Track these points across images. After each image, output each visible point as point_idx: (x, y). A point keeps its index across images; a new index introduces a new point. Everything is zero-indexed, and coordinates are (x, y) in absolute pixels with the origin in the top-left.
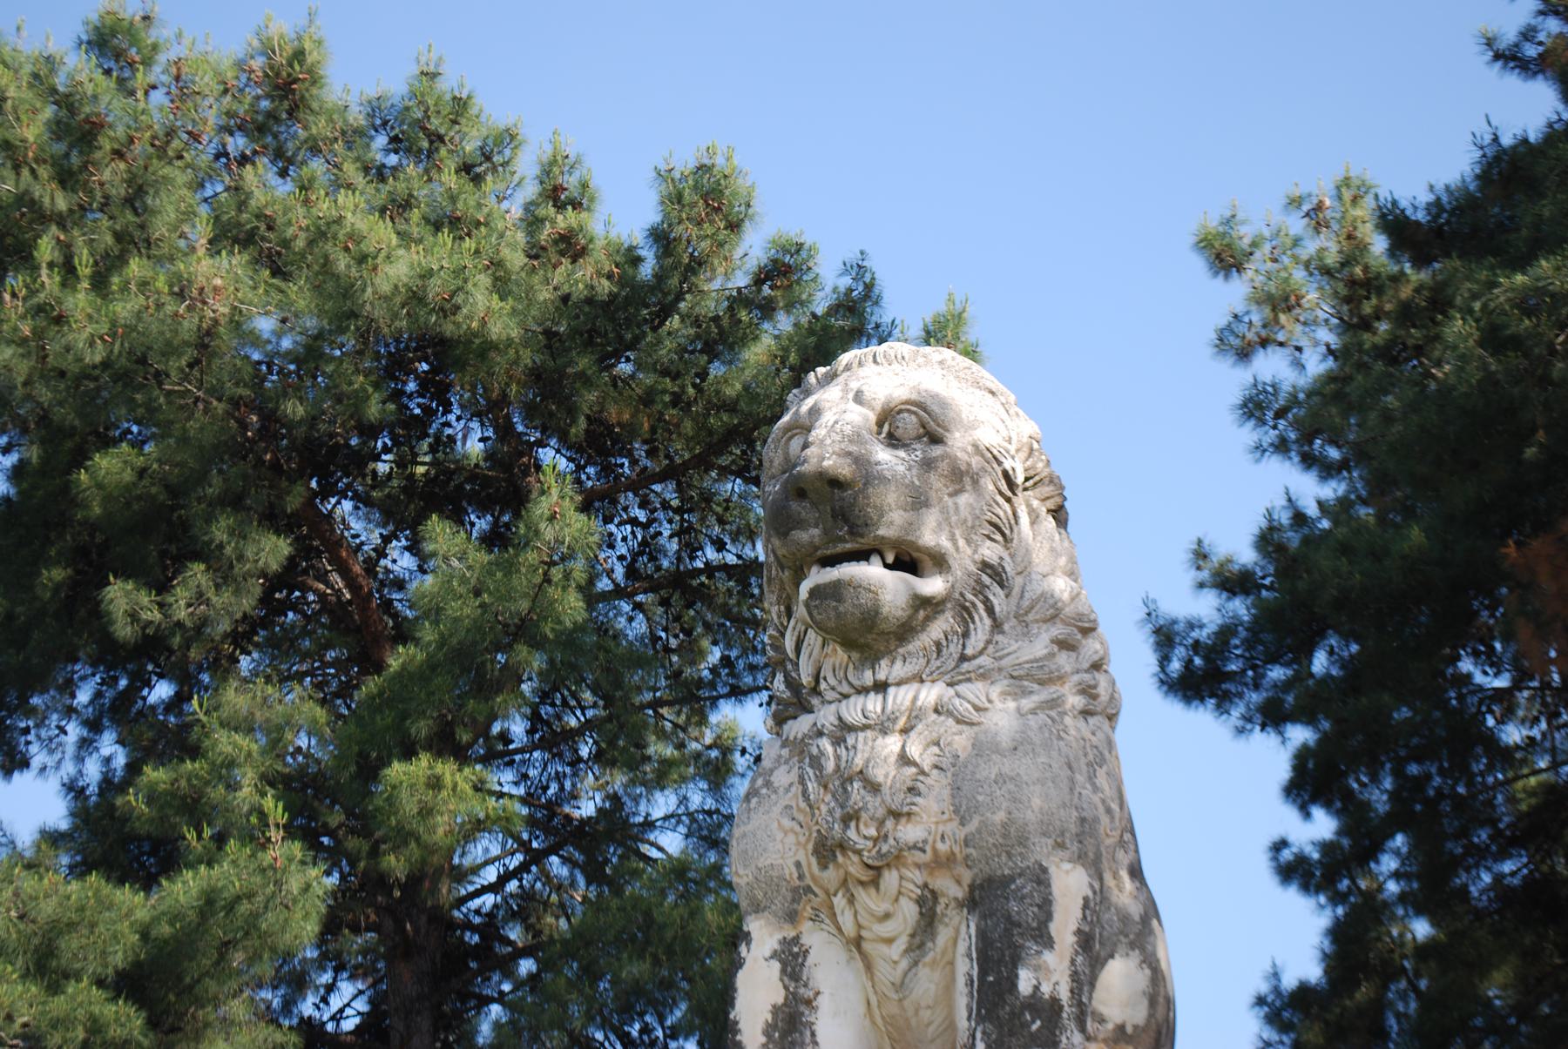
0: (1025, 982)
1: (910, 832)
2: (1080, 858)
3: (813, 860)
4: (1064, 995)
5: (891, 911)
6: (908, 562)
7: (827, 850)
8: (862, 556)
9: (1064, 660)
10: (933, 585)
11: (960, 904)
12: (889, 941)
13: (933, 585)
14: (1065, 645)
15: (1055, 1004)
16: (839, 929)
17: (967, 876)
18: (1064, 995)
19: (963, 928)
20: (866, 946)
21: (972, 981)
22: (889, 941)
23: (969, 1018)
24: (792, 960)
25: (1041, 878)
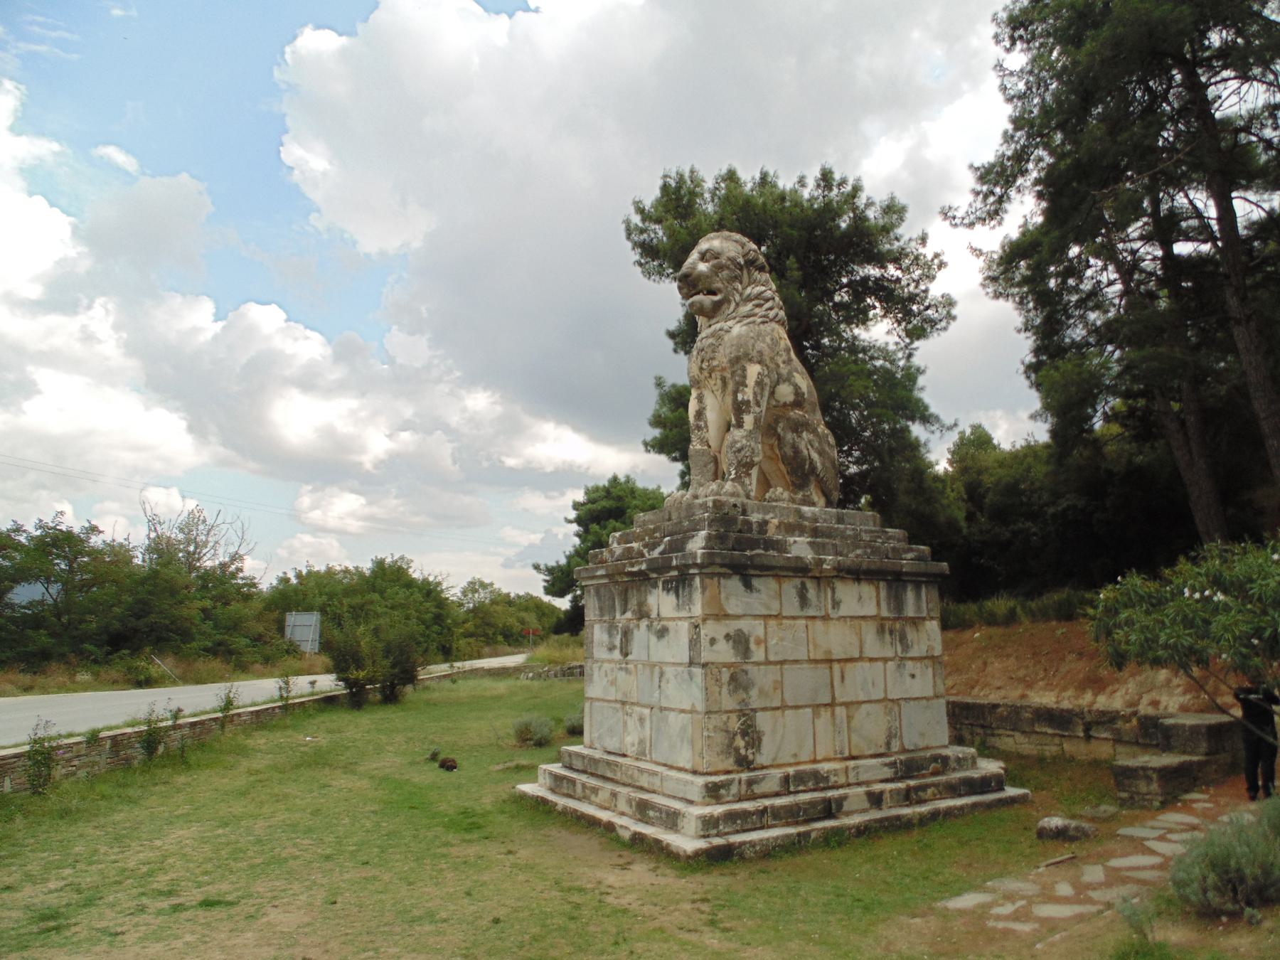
0: (740, 397)
1: (715, 363)
2: (759, 363)
4: (751, 398)
5: (715, 382)
6: (712, 292)
7: (701, 369)
8: (698, 293)
9: (757, 310)
10: (716, 298)
13: (716, 298)
14: (759, 306)
15: (748, 401)
18: (751, 398)
24: (700, 399)
25: (744, 369)
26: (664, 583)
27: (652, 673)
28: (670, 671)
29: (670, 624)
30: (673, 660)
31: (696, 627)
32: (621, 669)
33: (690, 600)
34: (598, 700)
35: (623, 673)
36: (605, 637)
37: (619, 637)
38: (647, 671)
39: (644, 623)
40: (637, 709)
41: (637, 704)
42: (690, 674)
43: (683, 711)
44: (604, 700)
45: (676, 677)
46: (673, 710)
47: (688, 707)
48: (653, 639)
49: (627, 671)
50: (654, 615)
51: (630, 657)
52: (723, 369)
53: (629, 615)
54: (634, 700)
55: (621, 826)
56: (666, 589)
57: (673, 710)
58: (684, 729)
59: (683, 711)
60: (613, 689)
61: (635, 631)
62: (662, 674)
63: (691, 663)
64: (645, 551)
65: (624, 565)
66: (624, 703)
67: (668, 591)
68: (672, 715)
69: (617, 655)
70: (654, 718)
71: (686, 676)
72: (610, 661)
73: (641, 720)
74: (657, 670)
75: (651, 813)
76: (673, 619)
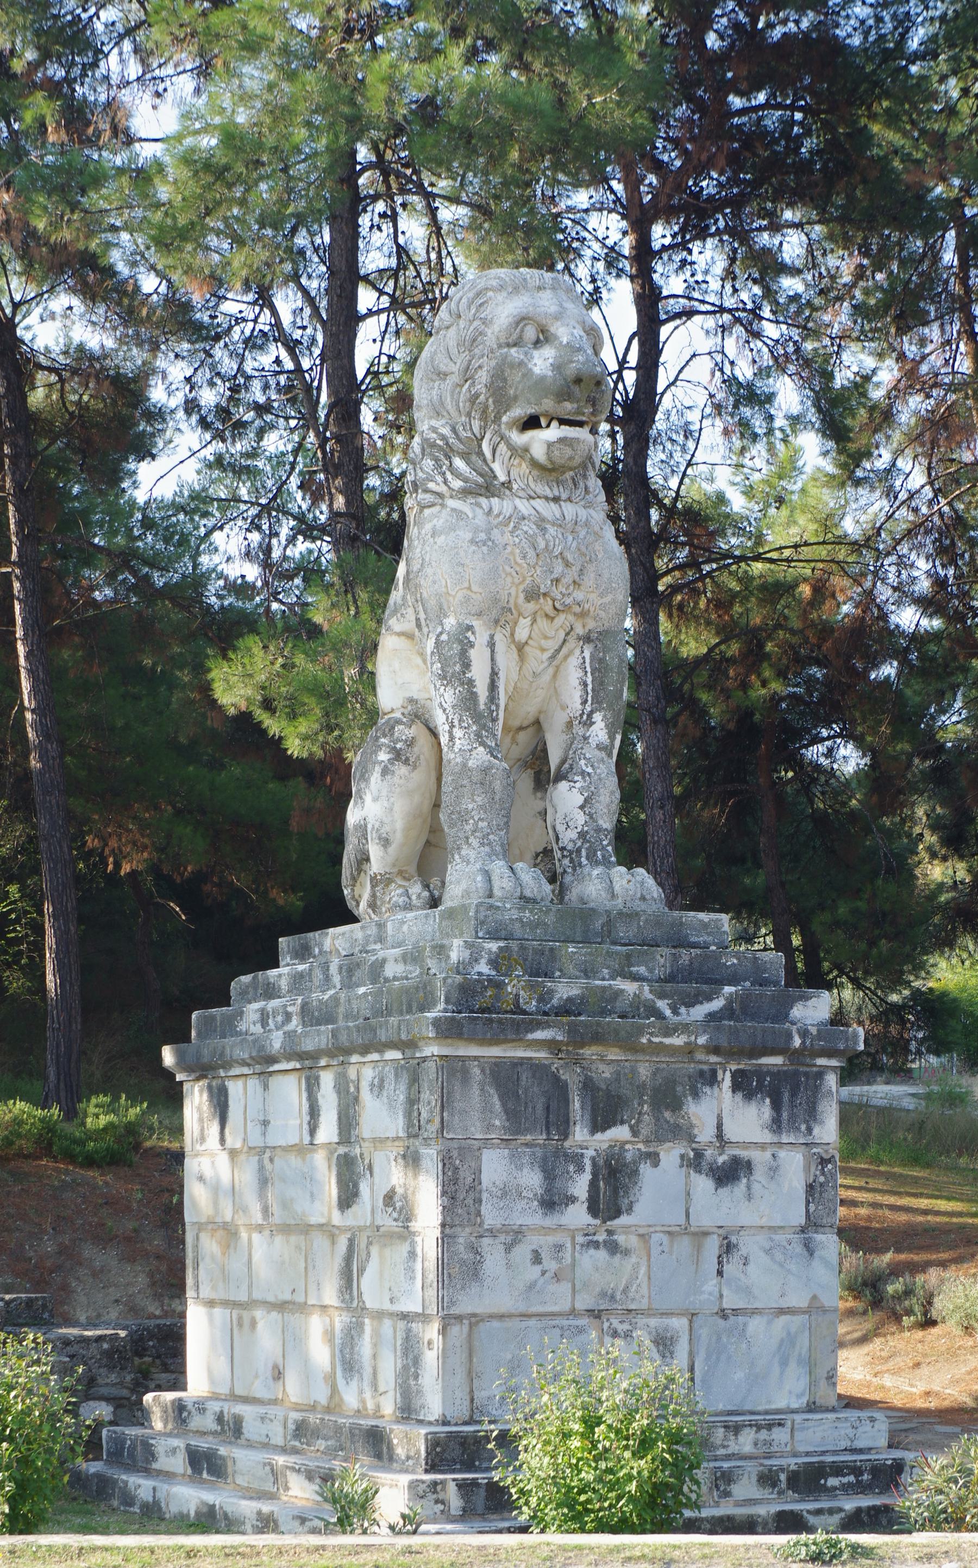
3: (522, 596)
11: (579, 639)
12: (543, 650)
16: (512, 635)
17: (591, 624)
19: (578, 652)
20: (527, 648)
21: (585, 685)
22: (543, 650)
23: (585, 702)
26: (734, 1075)
27: (699, 1249)
28: (749, 1245)
29: (760, 1158)
30: (764, 1222)
31: (823, 1162)
32: (596, 1245)
33: (812, 1115)
34: (501, 1317)
35: (602, 1254)
36: (532, 1179)
37: (587, 1177)
38: (685, 1244)
39: (671, 1155)
40: (653, 1322)
41: (649, 1312)
42: (810, 1249)
43: (782, 1311)
44: (525, 1316)
45: (768, 1252)
46: (755, 1312)
47: (804, 1304)
48: (703, 1184)
49: (613, 1248)
50: (705, 1134)
51: (623, 1220)
52: (583, 615)
53: (620, 1133)
54: (644, 1304)
55: (819, 1512)
56: (744, 1085)
57: (755, 1312)
58: (790, 1339)
59: (782, 1311)
60: (565, 1287)
61: (645, 1169)
62: (728, 1248)
63: (811, 1224)
64: (662, 1005)
65: (640, 1031)
66: (595, 1314)
67: (749, 1096)
68: (755, 1325)
69: (577, 1215)
70: (703, 1333)
71: (799, 1249)
72: (546, 1230)
73: (664, 1344)
74: (712, 1246)
75: (833, 1482)
76: (763, 1146)
